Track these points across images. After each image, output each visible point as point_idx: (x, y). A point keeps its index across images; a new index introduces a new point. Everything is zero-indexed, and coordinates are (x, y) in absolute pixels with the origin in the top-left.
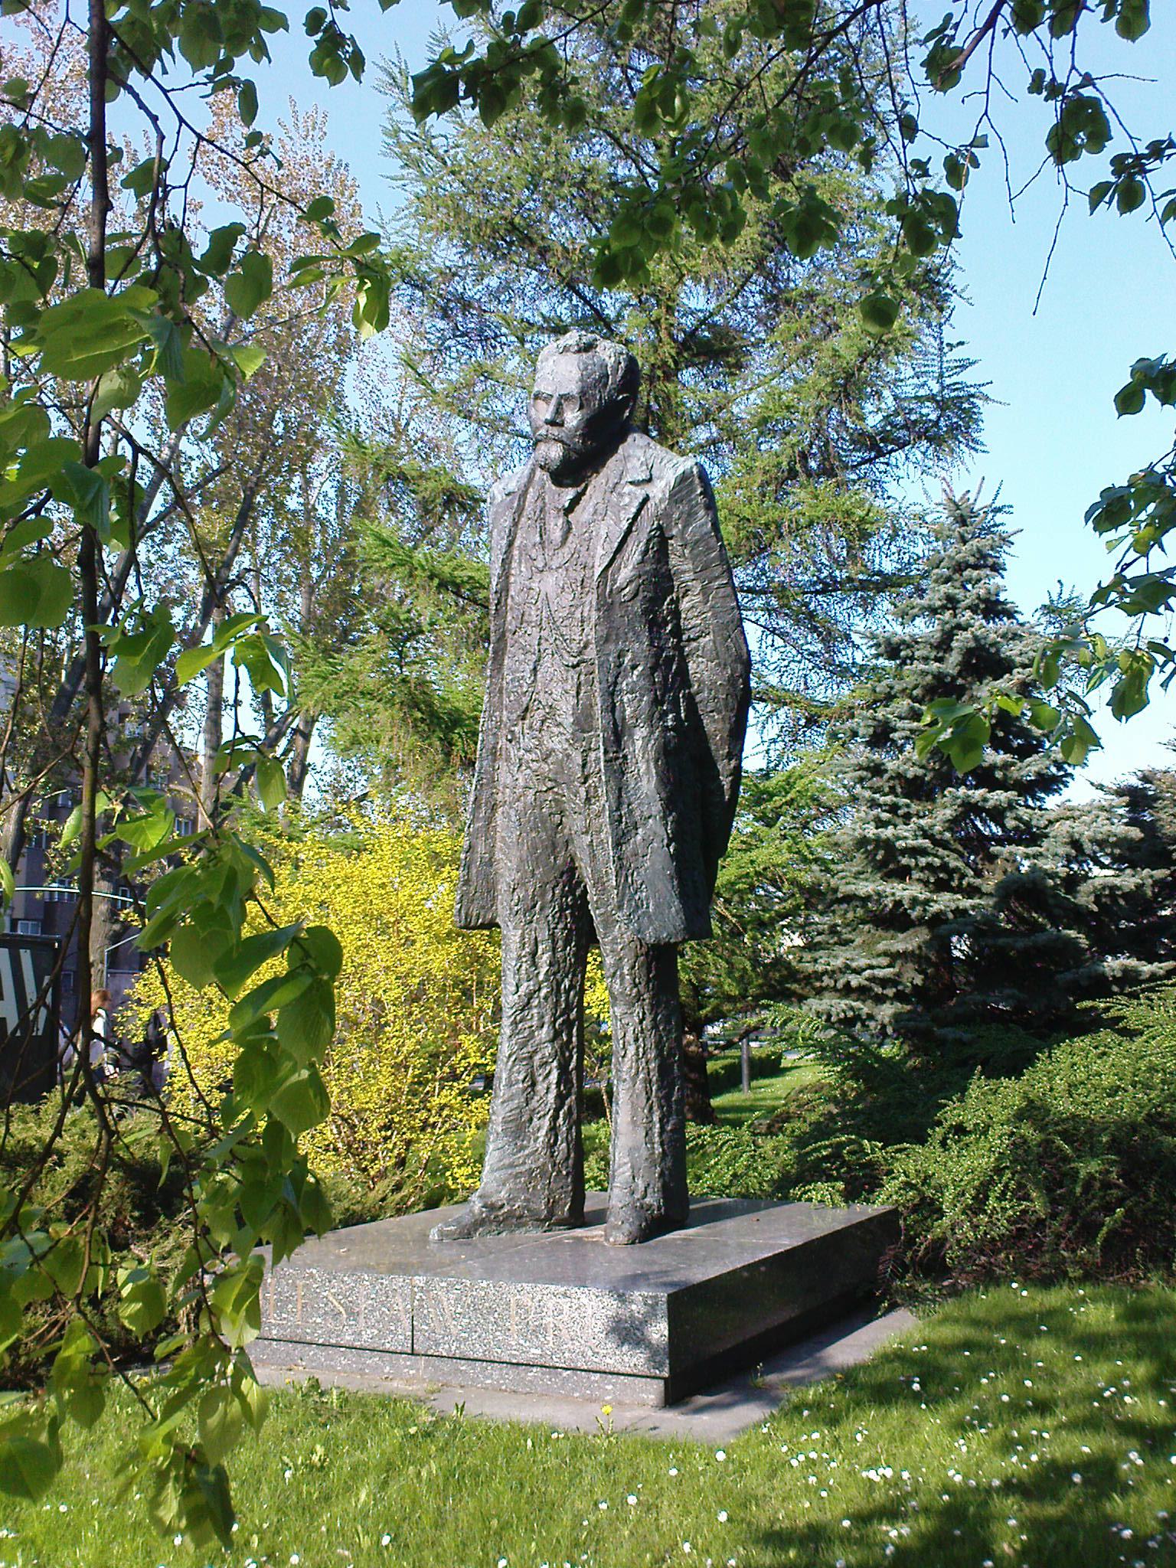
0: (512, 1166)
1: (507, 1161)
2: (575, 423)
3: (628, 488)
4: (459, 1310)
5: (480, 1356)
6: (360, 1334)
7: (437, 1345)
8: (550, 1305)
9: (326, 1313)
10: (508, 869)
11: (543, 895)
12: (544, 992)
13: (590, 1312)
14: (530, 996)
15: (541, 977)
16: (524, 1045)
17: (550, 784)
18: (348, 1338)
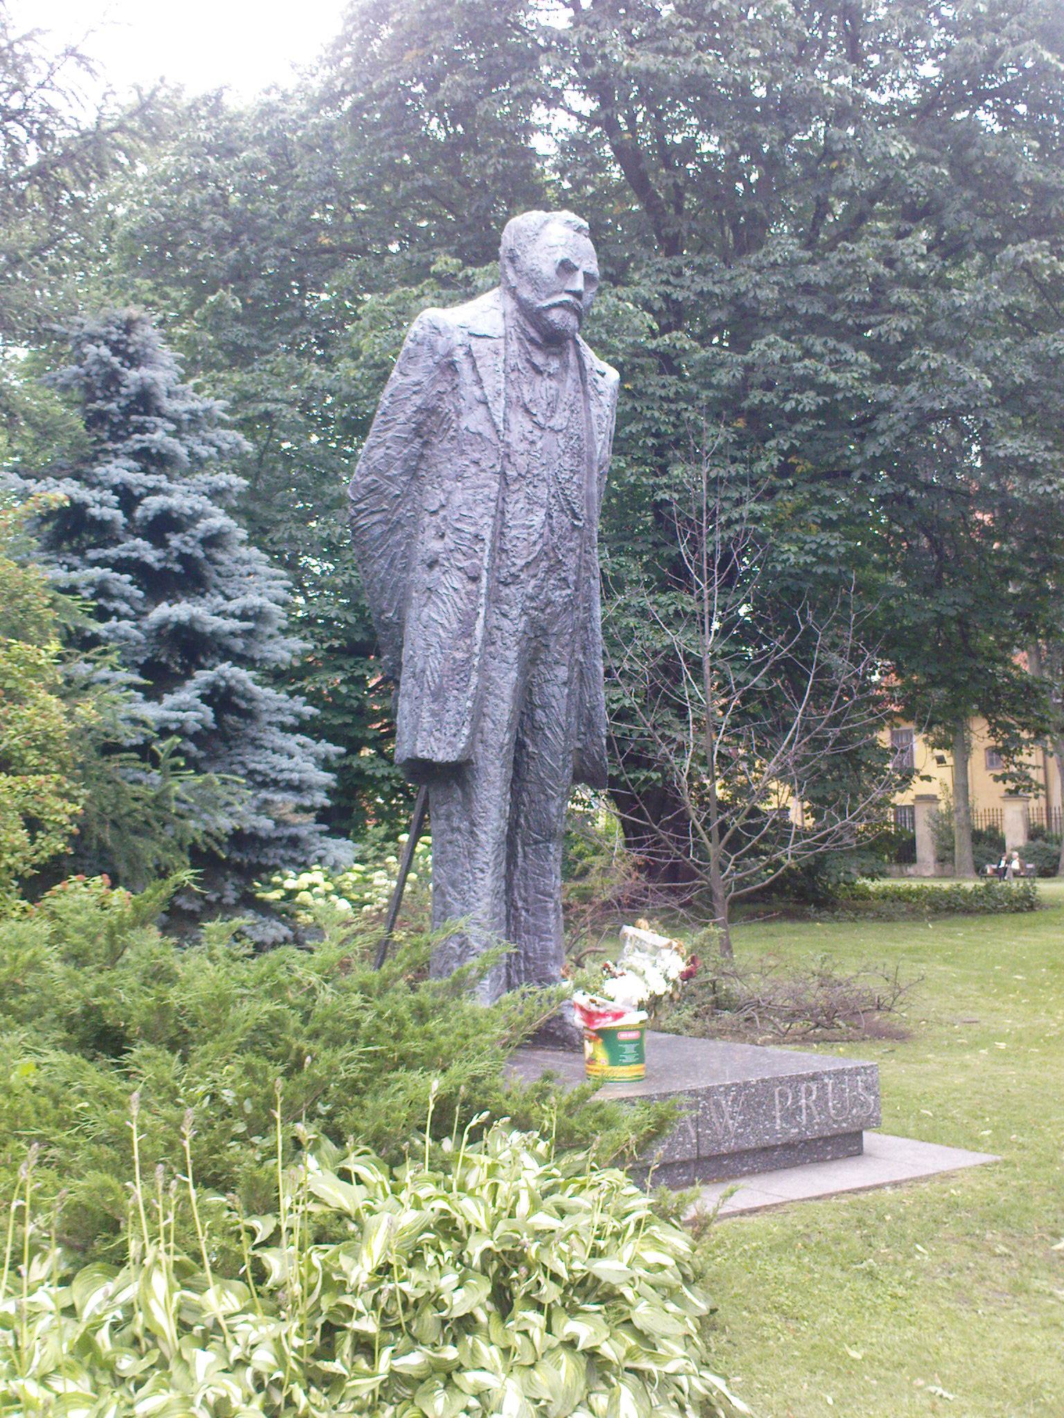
3: (598, 377)
8: (803, 1087)
10: (502, 709)
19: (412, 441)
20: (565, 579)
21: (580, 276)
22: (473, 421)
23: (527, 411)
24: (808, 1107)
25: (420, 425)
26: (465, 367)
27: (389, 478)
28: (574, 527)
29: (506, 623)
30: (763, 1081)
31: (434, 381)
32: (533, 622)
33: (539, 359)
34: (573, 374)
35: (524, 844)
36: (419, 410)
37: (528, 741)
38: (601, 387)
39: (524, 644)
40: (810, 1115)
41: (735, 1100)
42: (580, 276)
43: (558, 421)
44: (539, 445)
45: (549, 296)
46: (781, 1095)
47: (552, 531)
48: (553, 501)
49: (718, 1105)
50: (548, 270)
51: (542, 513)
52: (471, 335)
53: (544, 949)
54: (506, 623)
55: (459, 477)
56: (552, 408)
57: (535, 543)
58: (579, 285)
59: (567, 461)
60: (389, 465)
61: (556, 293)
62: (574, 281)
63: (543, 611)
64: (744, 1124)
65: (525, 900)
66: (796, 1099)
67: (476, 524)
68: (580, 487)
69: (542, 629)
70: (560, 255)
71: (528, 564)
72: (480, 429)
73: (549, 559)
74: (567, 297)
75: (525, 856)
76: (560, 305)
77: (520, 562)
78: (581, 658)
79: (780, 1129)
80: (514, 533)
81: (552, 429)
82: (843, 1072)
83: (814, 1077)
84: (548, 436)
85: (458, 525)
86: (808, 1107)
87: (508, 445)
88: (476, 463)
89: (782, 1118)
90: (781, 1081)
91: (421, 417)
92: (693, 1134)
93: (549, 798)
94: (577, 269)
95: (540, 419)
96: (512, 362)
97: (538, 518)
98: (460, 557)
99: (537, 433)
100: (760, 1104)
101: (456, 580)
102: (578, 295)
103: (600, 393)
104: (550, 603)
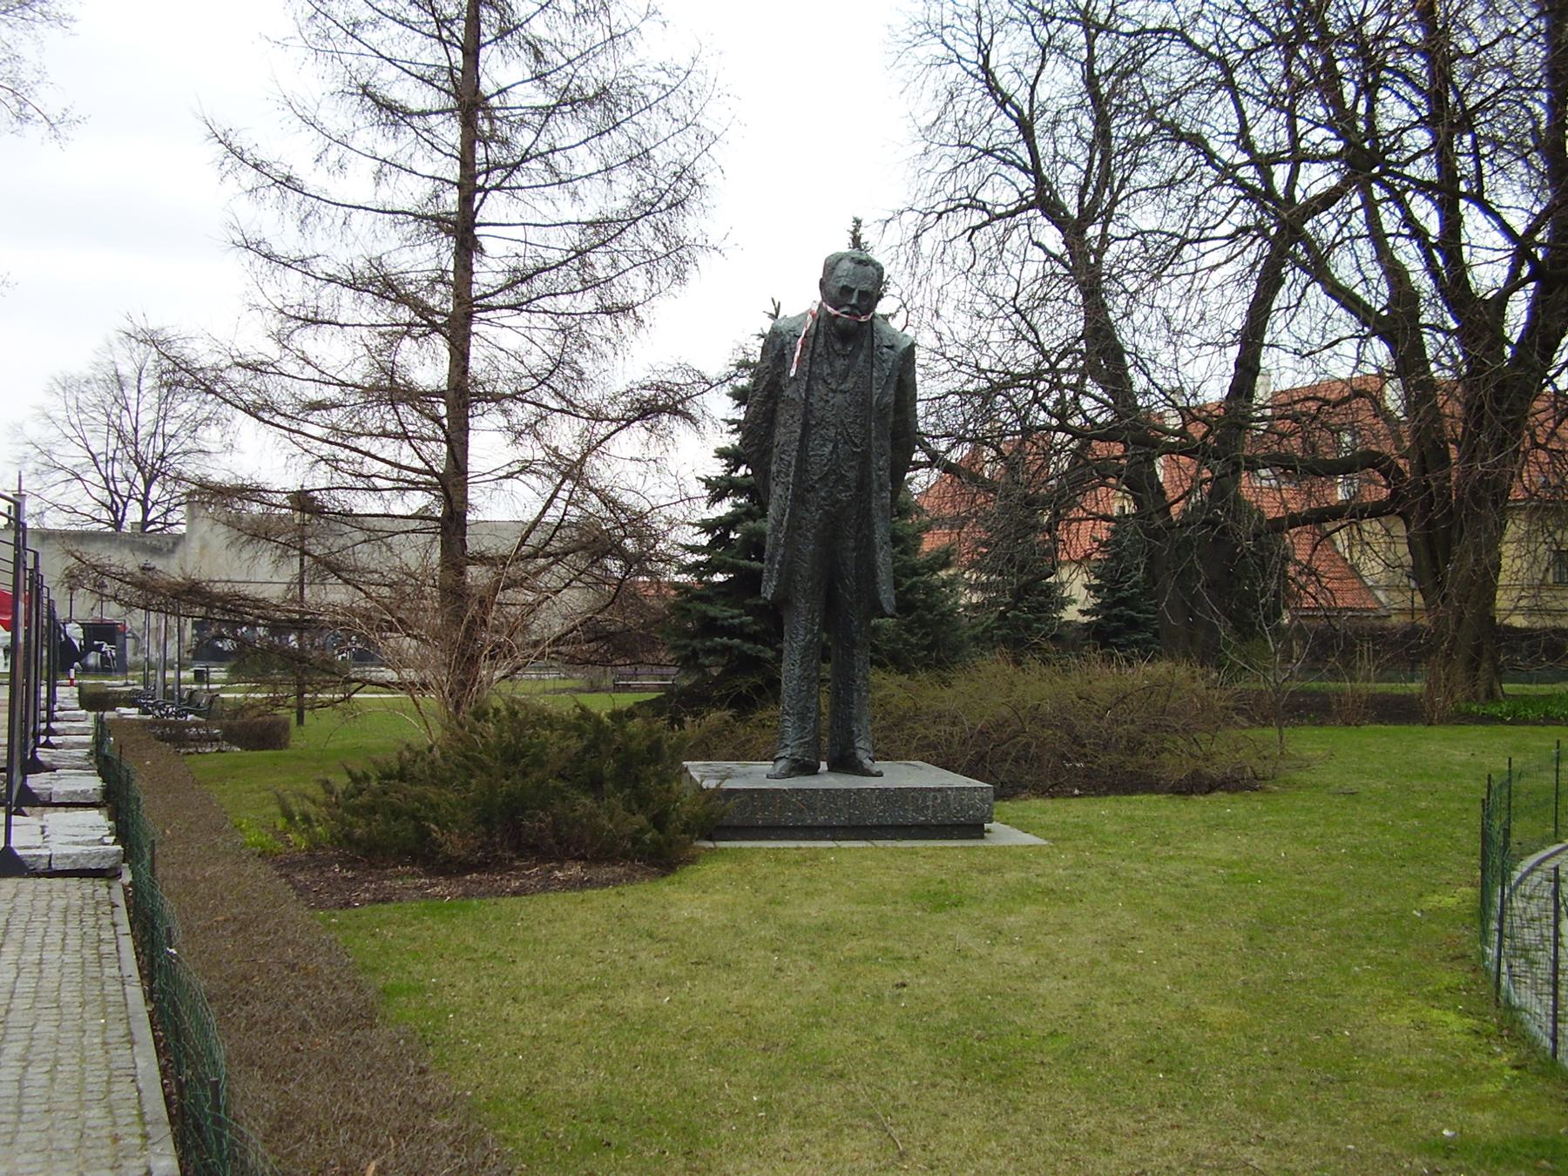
14: (811, 642)
21: (856, 294)
22: (788, 392)
29: (807, 515)
31: (775, 367)
32: (826, 513)
33: (838, 346)
42: (856, 294)
43: (848, 386)
50: (834, 292)
51: (830, 446)
54: (807, 515)
56: (844, 377)
58: (854, 301)
64: (884, 811)
66: (924, 801)
68: (862, 426)
70: (843, 282)
79: (911, 817)
83: (940, 790)
84: (840, 396)
95: (834, 386)
101: (779, 490)
102: (852, 306)
104: (839, 501)
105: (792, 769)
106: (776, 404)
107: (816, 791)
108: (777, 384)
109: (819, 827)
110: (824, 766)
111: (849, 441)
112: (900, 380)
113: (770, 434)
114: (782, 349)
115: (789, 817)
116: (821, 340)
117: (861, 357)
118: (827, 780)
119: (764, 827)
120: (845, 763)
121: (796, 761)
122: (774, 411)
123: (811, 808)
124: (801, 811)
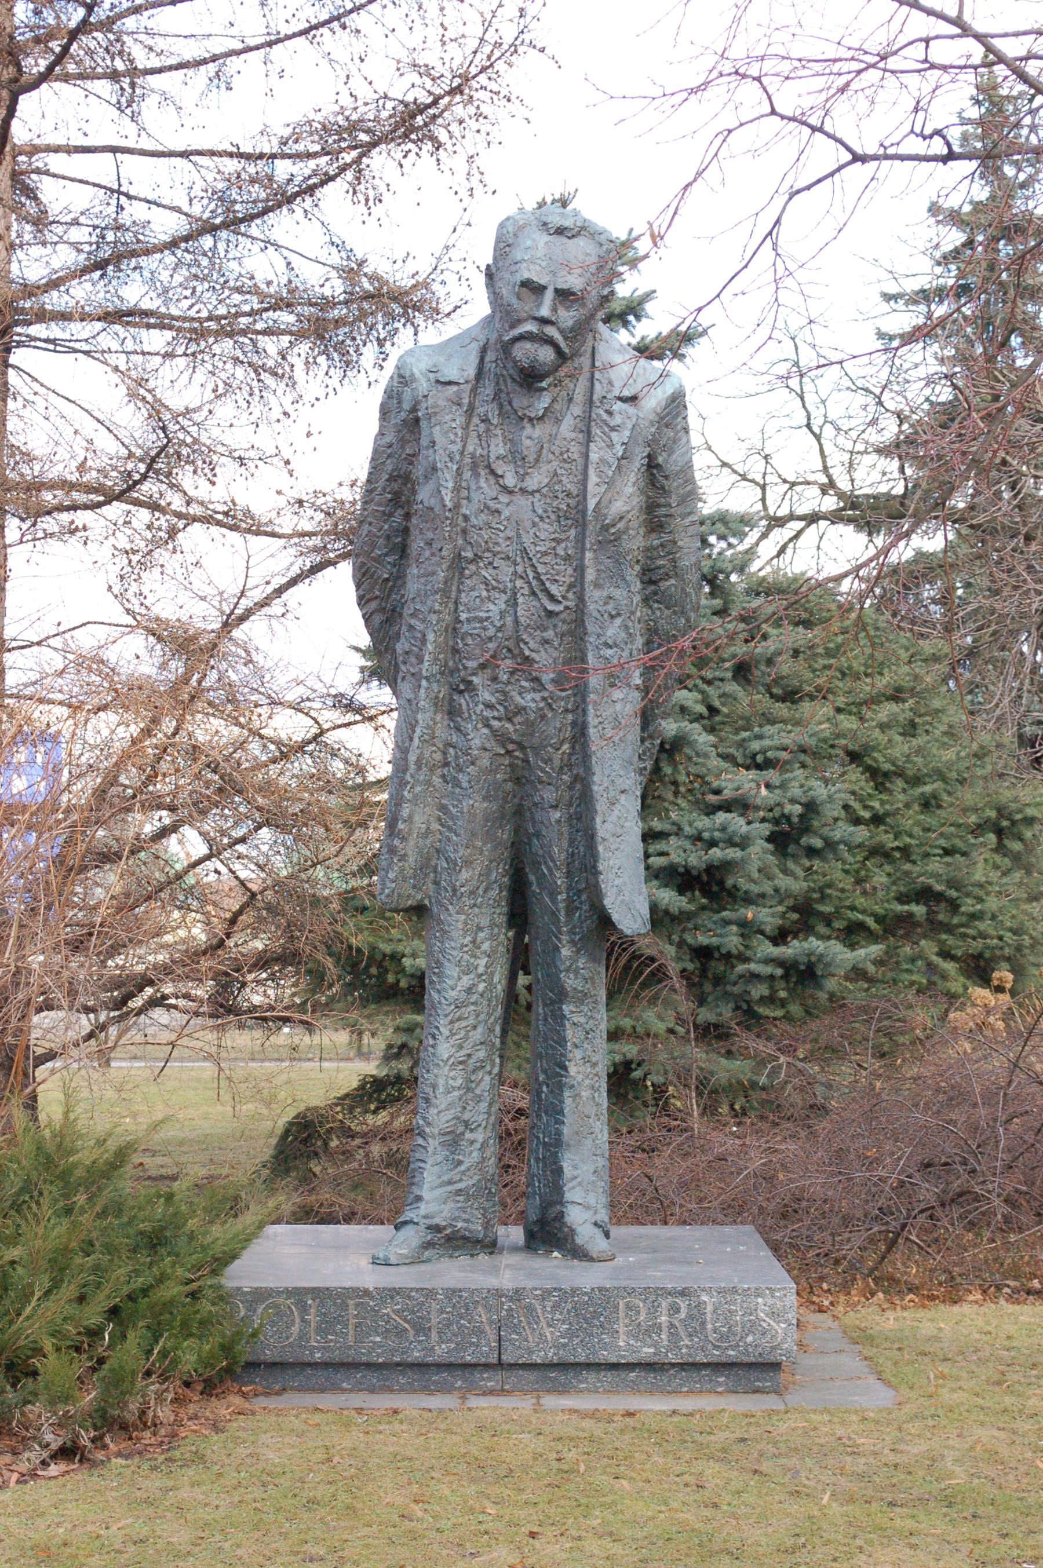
0: (450, 1183)
1: (445, 1178)
2: (570, 323)
3: (618, 406)
4: (558, 1316)
5: (582, 1359)
6: (432, 1349)
7: (530, 1352)
9: (387, 1331)
11: (488, 875)
12: (481, 987)
13: (709, 1308)
15: (481, 970)
16: (461, 1047)
17: (511, 747)
18: (416, 1355)
19: (391, 515)
20: (536, 680)
23: (493, 472)
24: (672, 1325)
25: (397, 495)
26: (424, 424)
27: (375, 560)
28: (550, 614)
30: (600, 1289)
31: (403, 442)
34: (577, 410)
35: (545, 1005)
36: (391, 479)
37: (532, 878)
38: (618, 420)
39: (485, 762)
40: (674, 1335)
41: (556, 1307)
44: (506, 513)
45: (513, 326)
46: (628, 1307)
47: (516, 621)
48: (519, 583)
49: (530, 1309)
52: (438, 381)
53: (559, 1133)
55: (419, 563)
57: (490, 639)
58: (545, 312)
59: (546, 529)
60: (373, 545)
61: (519, 322)
62: (539, 306)
63: (510, 720)
64: (570, 1334)
65: (545, 1071)
67: (423, 621)
69: (513, 742)
71: (483, 666)
72: (433, 502)
73: (514, 657)
74: (530, 327)
75: (546, 1020)
76: (521, 338)
77: (472, 664)
78: (581, 771)
80: (466, 627)
81: (523, 491)
82: (734, 1290)
83: (683, 1293)
85: (413, 622)
86: (672, 1325)
87: (466, 518)
88: (429, 544)
89: (629, 1334)
90: (631, 1292)
91: (395, 486)
92: (492, 1336)
93: (557, 949)
94: (545, 288)
95: (510, 481)
96: (481, 410)
97: (494, 610)
98: (413, 660)
99: (504, 498)
100: (596, 1315)
102: (544, 321)
103: (613, 429)
105: (428, 1245)
106: (407, 516)
107: (431, 1293)
108: (406, 478)
109: (440, 1366)
110: (516, 1234)
111: (540, 588)
112: (652, 465)
113: (398, 578)
114: (414, 409)
115: (376, 1347)
116: (488, 389)
117: (568, 422)
118: (513, 1271)
119: (326, 1365)
120: (547, 1233)
121: (437, 1229)
122: (406, 531)
123: (421, 1329)
124: (401, 1333)
